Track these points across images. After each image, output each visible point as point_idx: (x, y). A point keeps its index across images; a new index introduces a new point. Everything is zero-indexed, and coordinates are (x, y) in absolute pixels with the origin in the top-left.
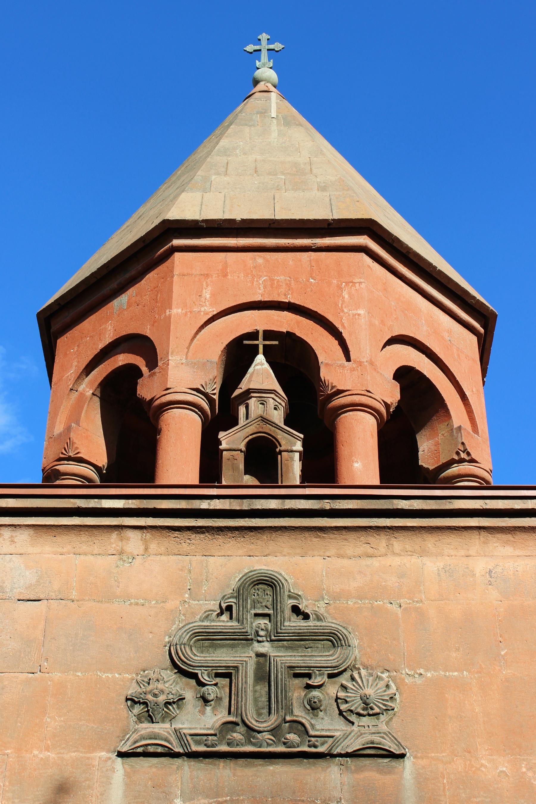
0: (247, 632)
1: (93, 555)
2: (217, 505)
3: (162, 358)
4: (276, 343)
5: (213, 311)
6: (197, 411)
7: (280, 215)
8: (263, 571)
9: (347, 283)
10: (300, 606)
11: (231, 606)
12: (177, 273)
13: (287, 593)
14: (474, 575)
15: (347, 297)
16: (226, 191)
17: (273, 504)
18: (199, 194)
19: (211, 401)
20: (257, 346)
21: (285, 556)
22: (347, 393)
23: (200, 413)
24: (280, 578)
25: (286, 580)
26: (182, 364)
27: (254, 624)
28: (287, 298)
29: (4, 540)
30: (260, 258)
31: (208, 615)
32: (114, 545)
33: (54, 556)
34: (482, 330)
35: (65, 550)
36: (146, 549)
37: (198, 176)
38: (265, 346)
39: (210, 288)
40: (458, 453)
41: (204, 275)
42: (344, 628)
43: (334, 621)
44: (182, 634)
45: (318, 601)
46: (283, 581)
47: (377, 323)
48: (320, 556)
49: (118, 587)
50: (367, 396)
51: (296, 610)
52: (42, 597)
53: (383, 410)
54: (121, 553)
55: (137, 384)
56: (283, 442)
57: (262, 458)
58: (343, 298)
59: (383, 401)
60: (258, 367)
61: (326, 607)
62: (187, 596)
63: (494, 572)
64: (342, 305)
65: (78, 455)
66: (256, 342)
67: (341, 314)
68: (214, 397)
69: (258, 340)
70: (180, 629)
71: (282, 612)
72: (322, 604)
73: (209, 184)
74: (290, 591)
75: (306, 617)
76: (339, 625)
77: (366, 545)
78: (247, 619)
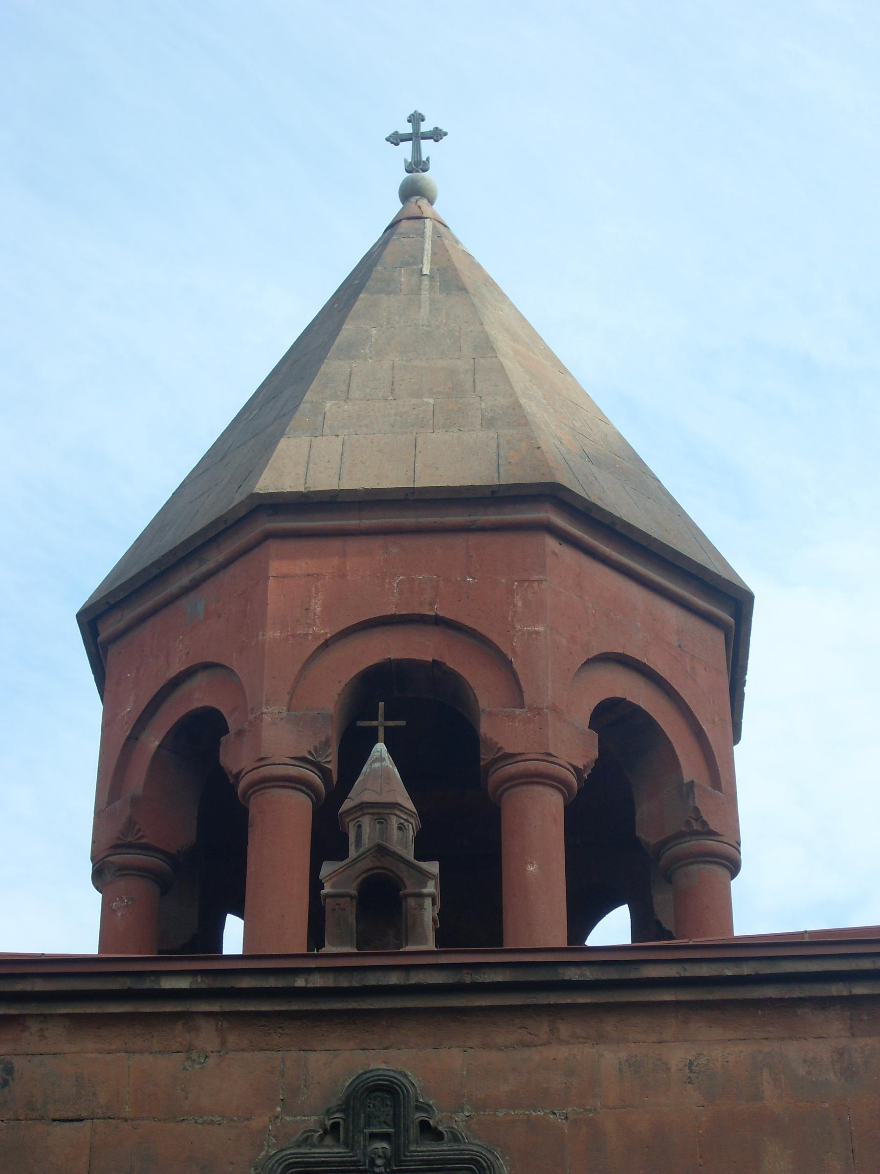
0: (358, 1161)
1: (152, 1053)
2: (317, 981)
3: (252, 709)
4: (403, 723)
5: (327, 633)
6: (304, 789)
7: (423, 481)
8: (381, 1072)
9: (521, 582)
10: (431, 1122)
11: (338, 1124)
12: (273, 574)
13: (413, 1103)
14: (669, 1069)
15: (520, 604)
16: (346, 432)
17: (394, 979)
18: (305, 440)
19: (324, 773)
20: (376, 729)
21: (412, 1048)
22: (519, 758)
23: (310, 792)
24: (405, 1081)
25: (413, 1084)
26: (282, 719)
27: (369, 1149)
28: (432, 609)
29: (31, 1034)
30: (395, 547)
31: (307, 1137)
32: (179, 1039)
33: (99, 1055)
34: (731, 620)
35: (113, 1047)
36: (223, 1043)
37: (307, 402)
38: (387, 729)
39: (321, 596)
40: (688, 823)
41: (312, 576)
42: (490, 1151)
43: (477, 1142)
44: (273, 1166)
45: (456, 1112)
46: (408, 1086)
47: (564, 641)
48: (458, 1047)
49: (186, 1098)
50: (548, 761)
51: (425, 1126)
52: (84, 1114)
53: (573, 780)
54: (189, 1049)
55: (218, 743)
56: (408, 883)
57: (381, 901)
58: (515, 606)
59: (571, 764)
60: (377, 765)
61: (466, 1121)
62: (279, 1109)
63: (695, 1064)
64: (512, 618)
65: (143, 841)
66: (375, 723)
67: (511, 632)
68: (329, 766)
69: (377, 720)
70: (270, 1158)
71: (407, 1130)
72: (459, 1117)
73: (320, 418)
74: (417, 1101)
75: (438, 1136)
76: (482, 1147)
77: (521, 1031)
78: (359, 1143)
